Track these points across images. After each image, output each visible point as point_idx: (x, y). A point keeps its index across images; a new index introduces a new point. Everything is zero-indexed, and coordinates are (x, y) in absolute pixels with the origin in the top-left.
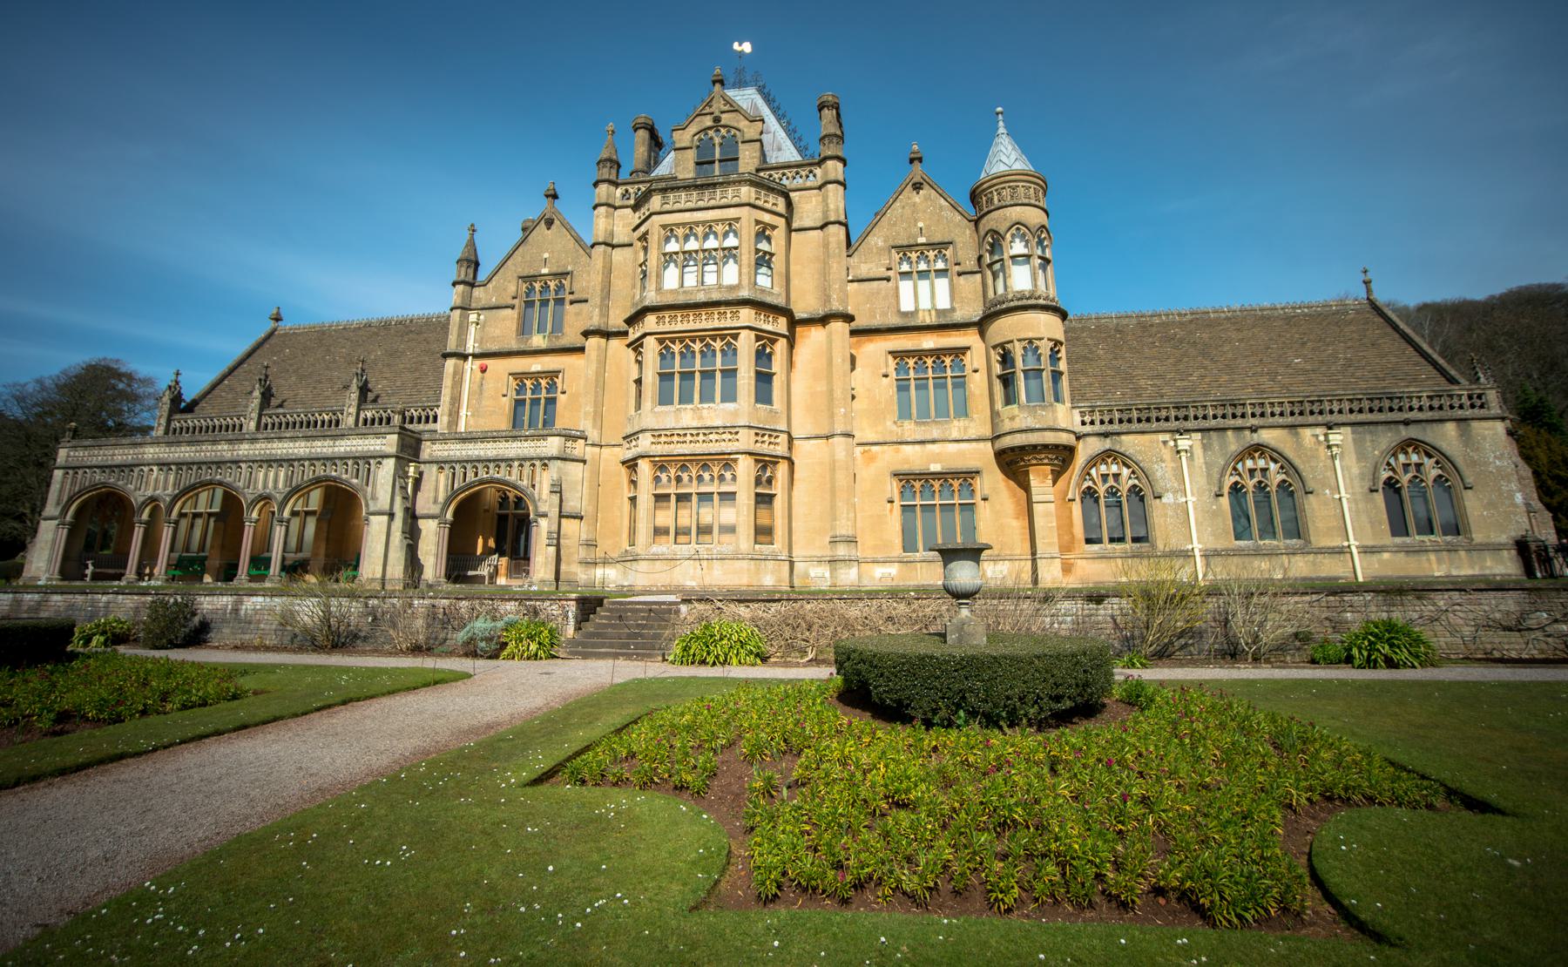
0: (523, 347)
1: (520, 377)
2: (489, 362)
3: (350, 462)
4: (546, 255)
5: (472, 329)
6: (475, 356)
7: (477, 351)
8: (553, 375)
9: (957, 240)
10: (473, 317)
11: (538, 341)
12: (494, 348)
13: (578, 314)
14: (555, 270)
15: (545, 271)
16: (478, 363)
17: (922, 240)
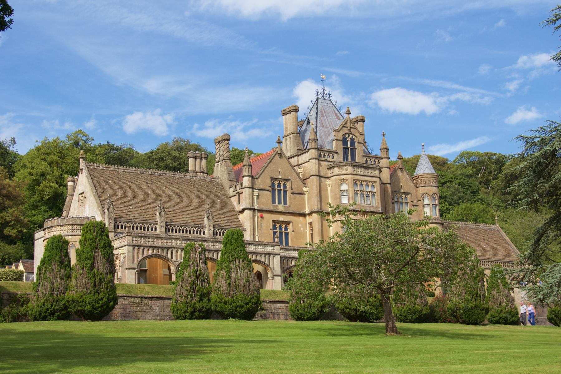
0: (275, 209)
1: (275, 222)
2: (265, 215)
3: (263, 255)
4: (280, 170)
5: (255, 199)
6: (258, 210)
7: (258, 208)
8: (289, 223)
9: (412, 192)
10: (256, 193)
11: (281, 208)
12: (264, 208)
13: (294, 198)
14: (284, 177)
15: (280, 177)
16: (259, 214)
17: (402, 191)
